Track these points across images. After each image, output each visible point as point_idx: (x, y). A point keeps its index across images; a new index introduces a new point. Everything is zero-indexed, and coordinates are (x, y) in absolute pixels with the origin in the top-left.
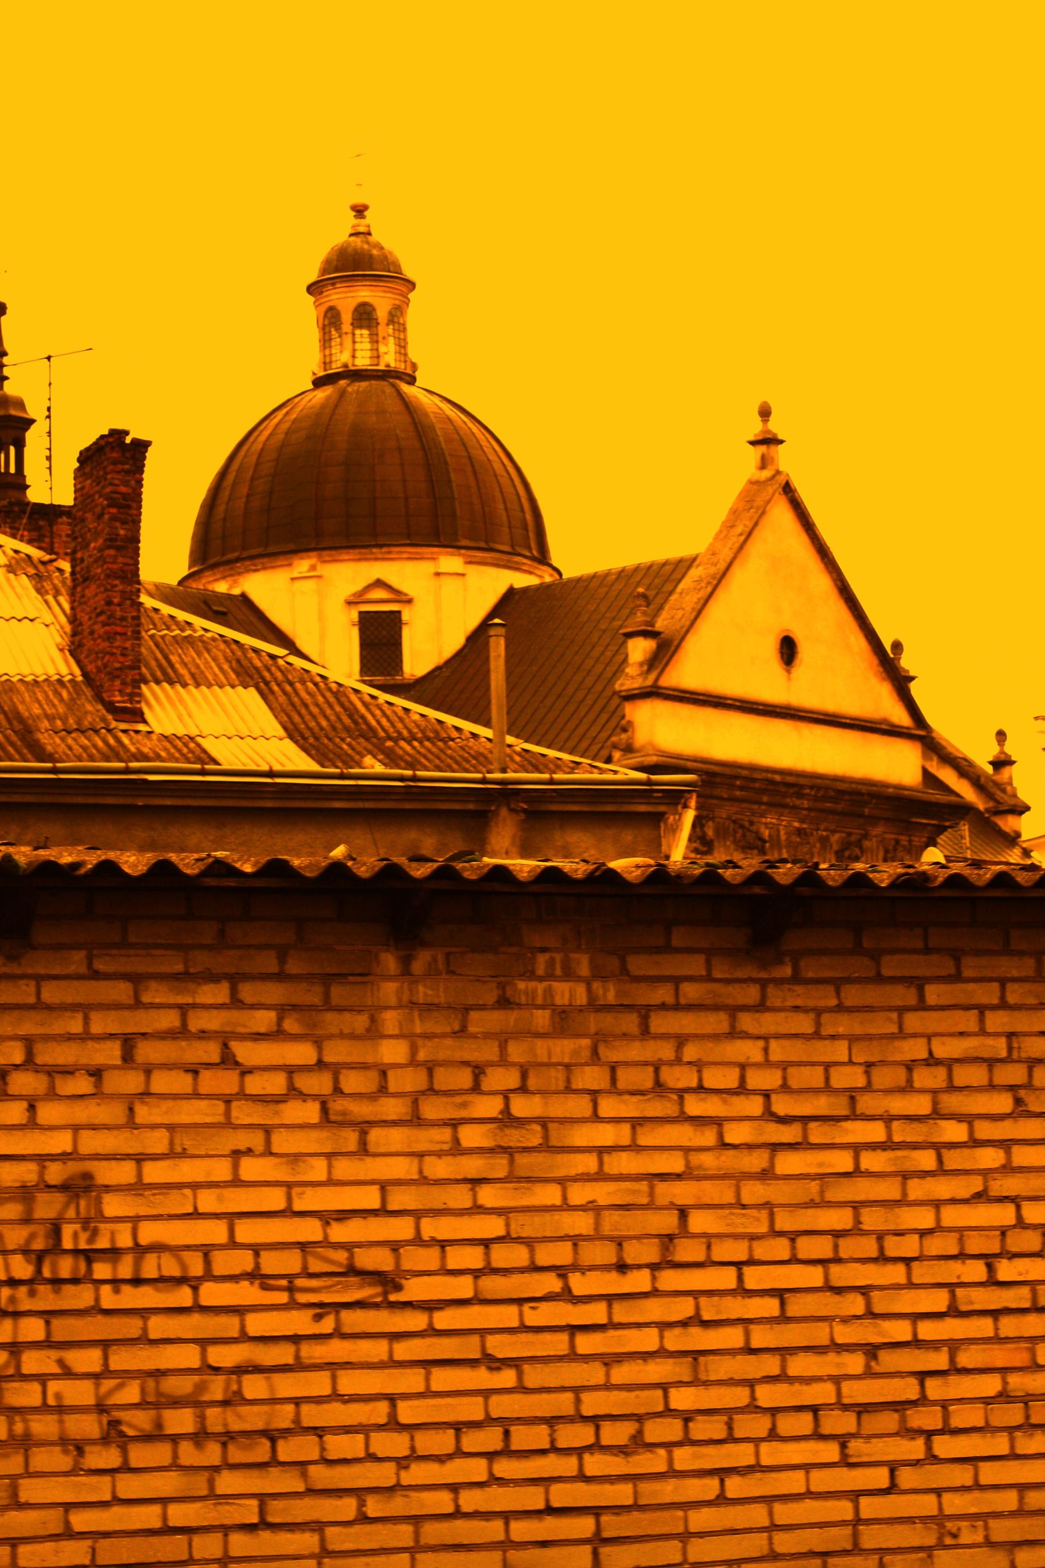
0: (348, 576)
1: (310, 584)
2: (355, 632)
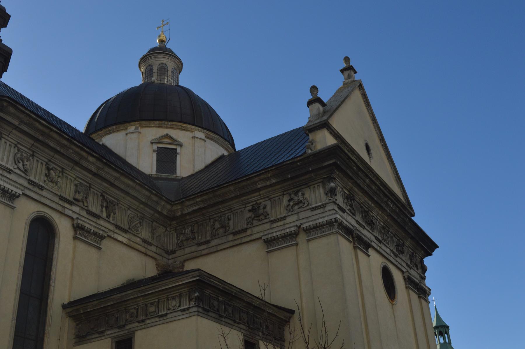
0: (153, 132)
1: (135, 136)
2: (155, 155)
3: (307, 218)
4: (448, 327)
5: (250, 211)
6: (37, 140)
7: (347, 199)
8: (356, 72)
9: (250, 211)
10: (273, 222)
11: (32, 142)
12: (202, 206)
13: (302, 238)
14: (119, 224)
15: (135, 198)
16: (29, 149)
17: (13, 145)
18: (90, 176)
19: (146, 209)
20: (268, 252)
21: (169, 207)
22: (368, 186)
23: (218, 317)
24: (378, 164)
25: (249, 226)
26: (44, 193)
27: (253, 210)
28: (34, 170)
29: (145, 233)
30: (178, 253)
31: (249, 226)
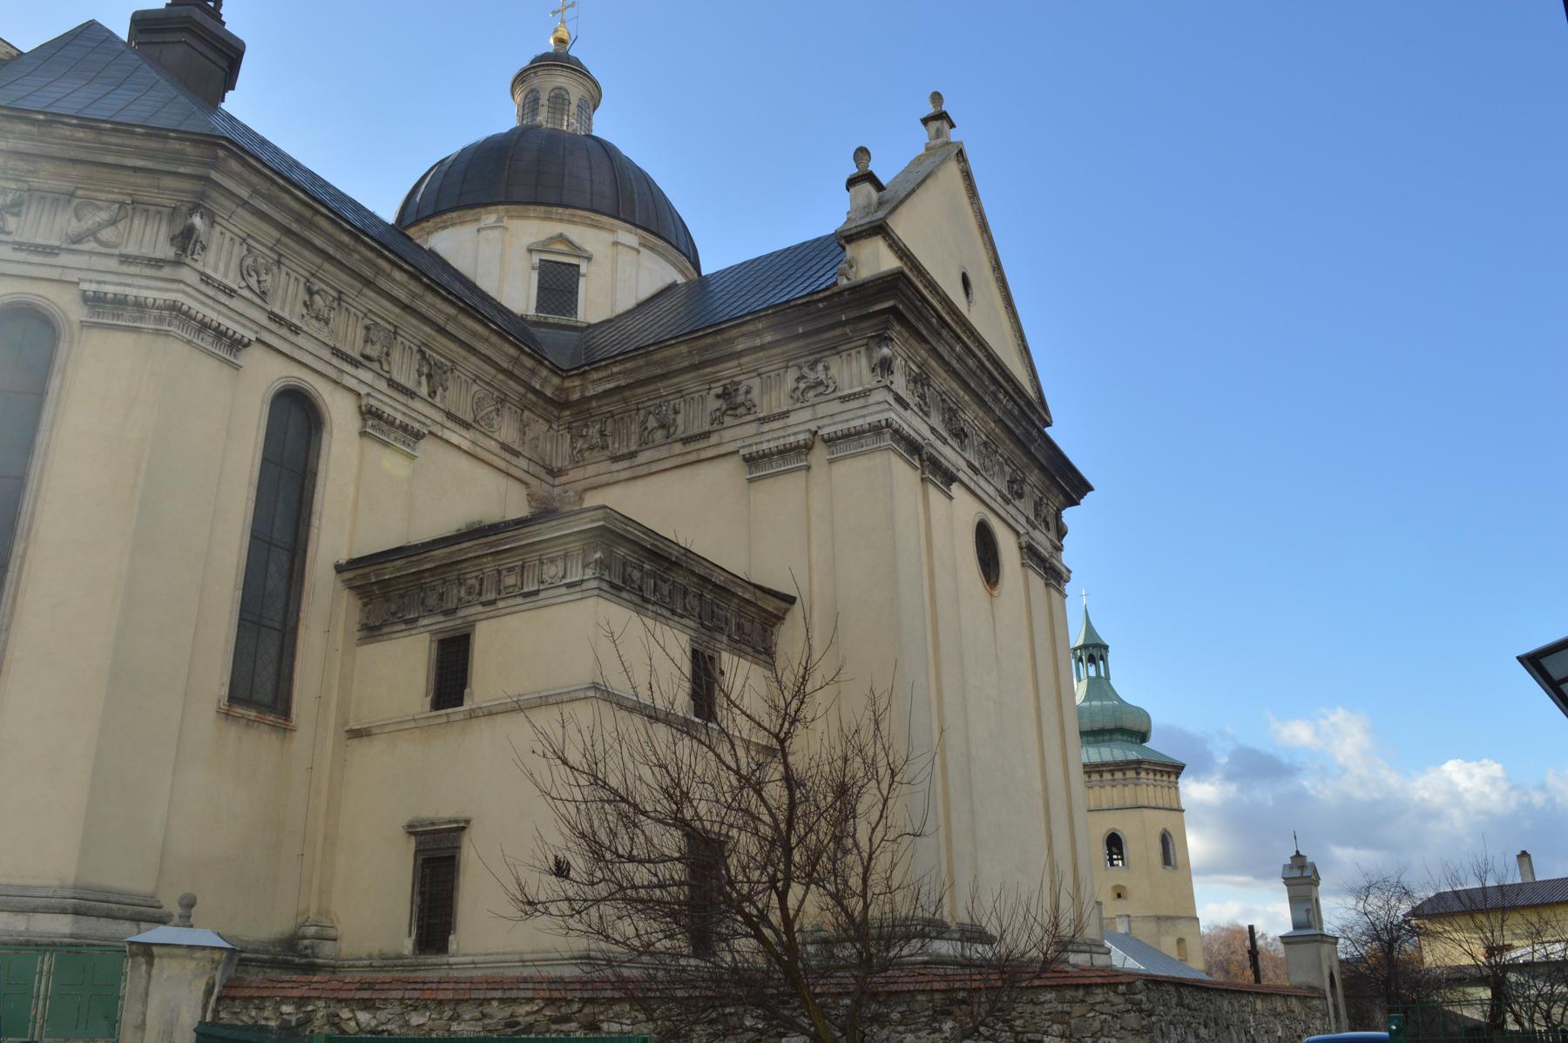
2: (535, 276)
3: (832, 417)
4: (1106, 648)
5: (718, 396)
6: (288, 232)
7: (915, 382)
8: (952, 126)
9: (718, 396)
10: (763, 420)
11: (277, 234)
12: (622, 383)
13: (819, 454)
14: (453, 410)
15: (487, 360)
16: (271, 249)
17: (238, 240)
18: (397, 310)
19: (511, 383)
20: (750, 481)
21: (556, 381)
22: (960, 359)
23: (639, 601)
24: (984, 316)
25: (715, 426)
26: (300, 340)
27: (725, 395)
28: (280, 293)
29: (507, 431)
30: (572, 475)
31: (715, 426)
